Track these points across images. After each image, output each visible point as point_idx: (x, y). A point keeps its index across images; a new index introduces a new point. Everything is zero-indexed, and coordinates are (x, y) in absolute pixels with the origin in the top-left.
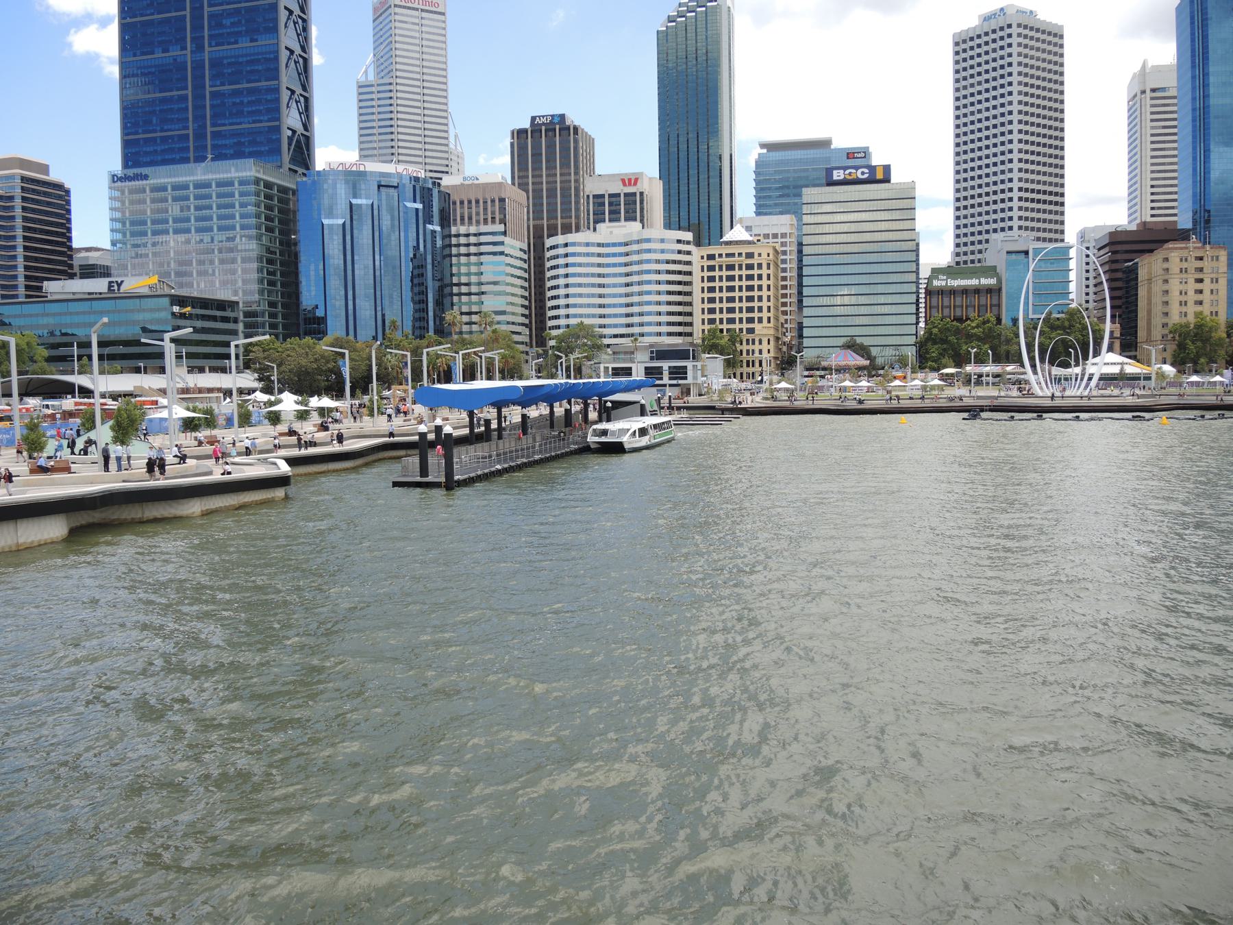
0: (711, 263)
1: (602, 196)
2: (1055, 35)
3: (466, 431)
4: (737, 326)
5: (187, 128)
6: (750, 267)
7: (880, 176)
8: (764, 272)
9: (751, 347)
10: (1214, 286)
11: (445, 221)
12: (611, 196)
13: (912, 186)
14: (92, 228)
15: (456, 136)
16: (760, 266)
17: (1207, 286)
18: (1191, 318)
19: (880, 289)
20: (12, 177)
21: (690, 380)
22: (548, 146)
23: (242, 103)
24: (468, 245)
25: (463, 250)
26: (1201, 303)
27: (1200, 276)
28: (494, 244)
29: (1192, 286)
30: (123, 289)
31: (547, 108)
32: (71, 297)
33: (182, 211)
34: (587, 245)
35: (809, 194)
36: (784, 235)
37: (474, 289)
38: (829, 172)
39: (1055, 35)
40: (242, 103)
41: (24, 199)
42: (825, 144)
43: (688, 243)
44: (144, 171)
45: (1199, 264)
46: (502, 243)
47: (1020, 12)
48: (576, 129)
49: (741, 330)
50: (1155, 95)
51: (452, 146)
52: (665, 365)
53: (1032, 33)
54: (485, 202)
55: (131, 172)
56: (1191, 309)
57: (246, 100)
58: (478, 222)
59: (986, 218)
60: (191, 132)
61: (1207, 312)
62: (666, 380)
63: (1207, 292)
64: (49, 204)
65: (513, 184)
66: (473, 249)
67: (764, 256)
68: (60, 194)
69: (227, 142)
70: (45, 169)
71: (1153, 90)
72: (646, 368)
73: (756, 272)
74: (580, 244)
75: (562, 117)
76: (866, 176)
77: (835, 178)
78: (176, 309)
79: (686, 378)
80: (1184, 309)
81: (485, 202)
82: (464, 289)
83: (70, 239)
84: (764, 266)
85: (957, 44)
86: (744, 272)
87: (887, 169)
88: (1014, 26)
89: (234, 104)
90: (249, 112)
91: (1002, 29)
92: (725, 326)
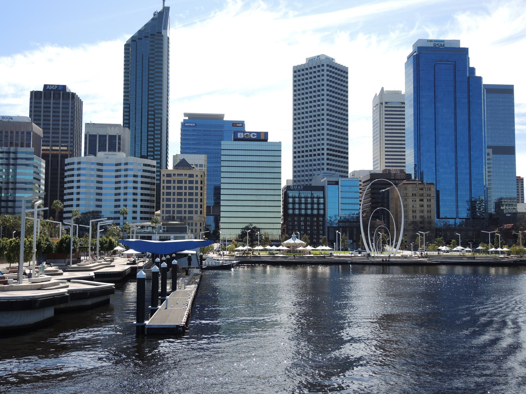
0: (169, 179)
1: (95, 136)
2: (344, 72)
4: (183, 215)
6: (191, 182)
7: (262, 137)
10: (429, 203)
12: (100, 136)
17: (425, 203)
18: (418, 219)
19: (263, 198)
26: (422, 212)
27: (422, 198)
28: (27, 159)
29: (418, 203)
31: (55, 80)
36: (201, 166)
38: (235, 133)
39: (344, 72)
42: (219, 117)
43: (154, 166)
45: (421, 192)
46: (32, 159)
47: (328, 58)
48: (73, 95)
49: (185, 217)
50: (386, 105)
53: (334, 70)
56: (418, 214)
59: (310, 163)
61: (426, 216)
63: (425, 206)
67: (199, 176)
71: (386, 103)
73: (194, 185)
77: (239, 137)
80: (415, 214)
84: (199, 182)
85: (295, 72)
86: (188, 185)
87: (266, 134)
88: (325, 65)
91: (319, 66)
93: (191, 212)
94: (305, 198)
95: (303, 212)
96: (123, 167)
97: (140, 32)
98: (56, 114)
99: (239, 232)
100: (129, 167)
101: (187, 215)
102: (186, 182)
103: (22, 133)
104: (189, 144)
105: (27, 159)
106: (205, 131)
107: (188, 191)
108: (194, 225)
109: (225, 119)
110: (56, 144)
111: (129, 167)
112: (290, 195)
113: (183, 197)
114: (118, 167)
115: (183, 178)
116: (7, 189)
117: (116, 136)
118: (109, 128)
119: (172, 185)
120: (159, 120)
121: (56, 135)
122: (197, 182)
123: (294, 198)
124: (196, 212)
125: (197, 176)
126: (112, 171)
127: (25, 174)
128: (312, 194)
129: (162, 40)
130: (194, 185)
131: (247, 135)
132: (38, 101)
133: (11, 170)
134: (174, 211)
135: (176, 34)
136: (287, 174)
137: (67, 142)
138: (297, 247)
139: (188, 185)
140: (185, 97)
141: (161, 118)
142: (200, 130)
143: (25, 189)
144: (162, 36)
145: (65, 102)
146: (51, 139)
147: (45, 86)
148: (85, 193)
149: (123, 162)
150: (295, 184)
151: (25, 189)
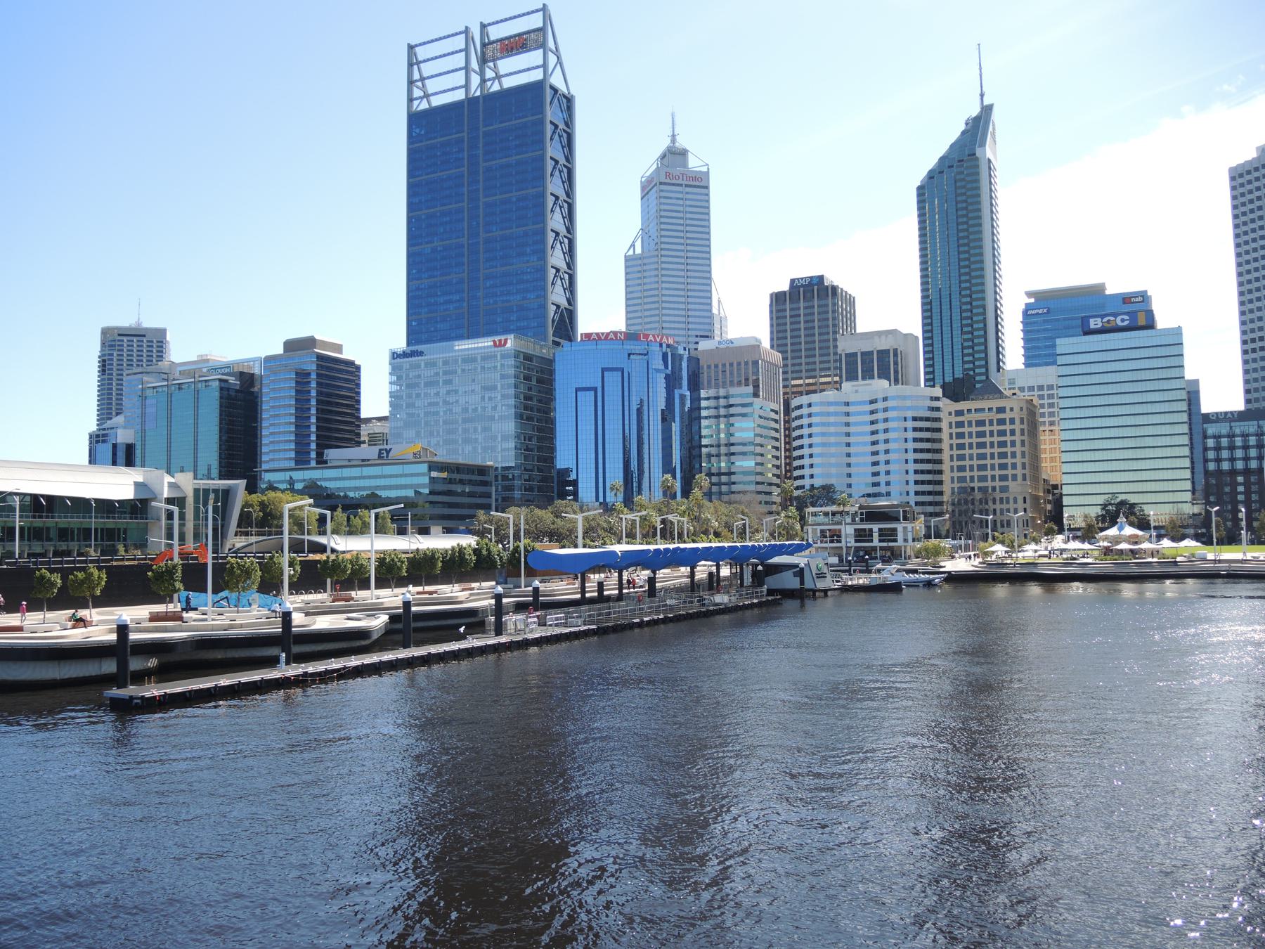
0: (960, 419)
3: (579, 596)
4: (989, 484)
6: (1001, 422)
7: (1142, 322)
8: (1017, 427)
9: (1005, 506)
11: (695, 385)
13: (1178, 331)
14: (375, 399)
16: (1012, 421)
22: (809, 307)
28: (743, 405)
32: (346, 463)
35: (1063, 344)
38: (1085, 321)
42: (1096, 291)
44: (420, 348)
48: (834, 289)
51: (715, 311)
52: (875, 528)
55: (413, 348)
65: (772, 347)
67: (1016, 409)
68: (351, 372)
70: (339, 348)
73: (1008, 427)
75: (821, 278)
76: (1126, 323)
77: (1092, 326)
79: (896, 541)
83: (358, 410)
84: (1017, 421)
85: (1233, 179)
86: (995, 428)
92: (976, 485)
93: (1004, 478)
94: (1243, 436)
95: (1240, 465)
96: (880, 405)
97: (942, 159)
98: (810, 325)
99: (1098, 511)
100: (889, 404)
101: (997, 484)
102: (991, 423)
103: (746, 363)
104: (1038, 348)
105: (743, 405)
106: (1071, 316)
107: (996, 439)
108: (1011, 501)
109: (1107, 292)
110: (813, 374)
111: (889, 404)
112: (1210, 432)
113: (988, 451)
114: (874, 407)
115: (985, 416)
116: (718, 455)
117: (887, 351)
118: (876, 339)
119: (966, 430)
120: (981, 310)
121: (811, 360)
122: (1012, 421)
123: (1217, 437)
124: (1014, 477)
125: (1012, 409)
126: (864, 413)
127: (742, 430)
128: (1259, 426)
129: (977, 166)
130: (1008, 427)
131: (1108, 322)
132: (781, 307)
133: (722, 426)
134: (972, 478)
135: (1002, 153)
136: (1222, 387)
137: (829, 369)
138: (1118, 543)
139: (995, 428)
140: (1027, 264)
141: (984, 307)
142: (1058, 320)
143: (744, 454)
144: (977, 159)
145: (822, 302)
146: (803, 367)
147: (792, 281)
148: (821, 455)
149: (880, 396)
150: (1250, 406)
151: (744, 454)
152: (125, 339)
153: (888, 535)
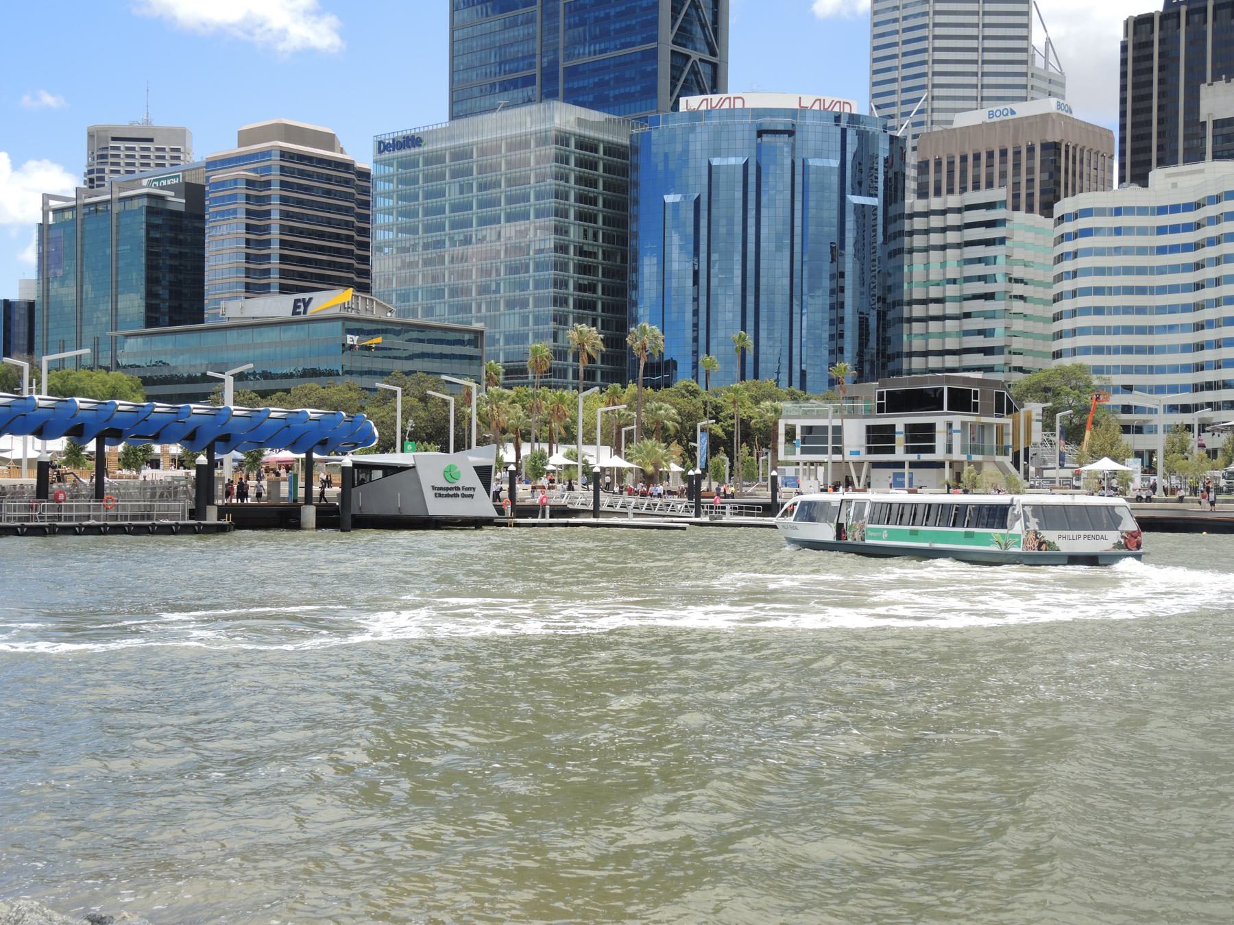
5: (532, 66)
15: (1048, 42)
20: (265, 154)
21: (939, 455)
23: (607, 17)
24: (944, 230)
25: (935, 239)
30: (311, 310)
33: (461, 192)
34: (1118, 211)
37: (951, 308)
40: (607, 17)
41: (283, 184)
51: (1039, 62)
52: (900, 422)
54: (1017, 153)
57: (612, 12)
58: (963, 189)
60: (537, 71)
62: (900, 455)
64: (328, 193)
66: (952, 237)
69: (586, 83)
70: (329, 140)
72: (868, 427)
74: (1101, 212)
78: (352, 339)
79: (931, 450)
81: (1017, 153)
82: (934, 309)
89: (597, 20)
90: (617, 31)
152: (122, 145)
153: (921, 437)
